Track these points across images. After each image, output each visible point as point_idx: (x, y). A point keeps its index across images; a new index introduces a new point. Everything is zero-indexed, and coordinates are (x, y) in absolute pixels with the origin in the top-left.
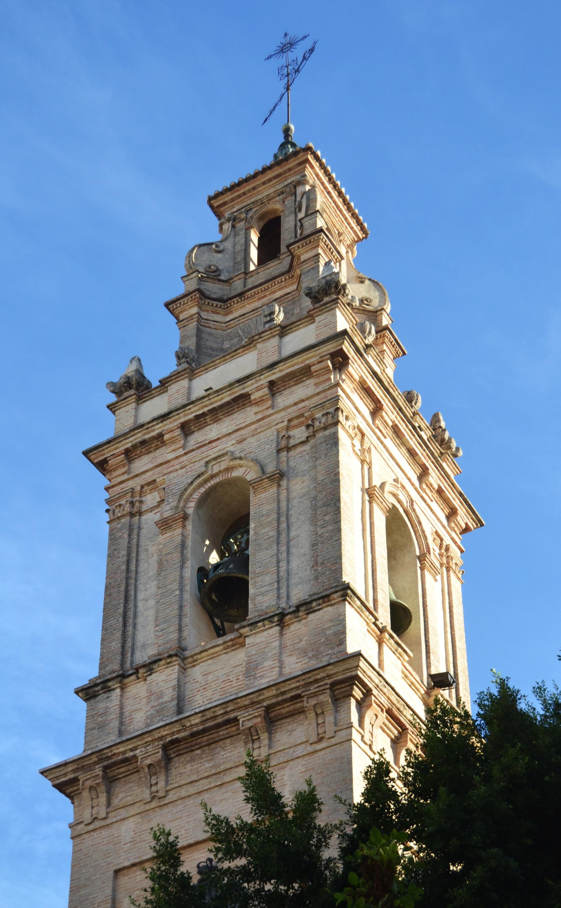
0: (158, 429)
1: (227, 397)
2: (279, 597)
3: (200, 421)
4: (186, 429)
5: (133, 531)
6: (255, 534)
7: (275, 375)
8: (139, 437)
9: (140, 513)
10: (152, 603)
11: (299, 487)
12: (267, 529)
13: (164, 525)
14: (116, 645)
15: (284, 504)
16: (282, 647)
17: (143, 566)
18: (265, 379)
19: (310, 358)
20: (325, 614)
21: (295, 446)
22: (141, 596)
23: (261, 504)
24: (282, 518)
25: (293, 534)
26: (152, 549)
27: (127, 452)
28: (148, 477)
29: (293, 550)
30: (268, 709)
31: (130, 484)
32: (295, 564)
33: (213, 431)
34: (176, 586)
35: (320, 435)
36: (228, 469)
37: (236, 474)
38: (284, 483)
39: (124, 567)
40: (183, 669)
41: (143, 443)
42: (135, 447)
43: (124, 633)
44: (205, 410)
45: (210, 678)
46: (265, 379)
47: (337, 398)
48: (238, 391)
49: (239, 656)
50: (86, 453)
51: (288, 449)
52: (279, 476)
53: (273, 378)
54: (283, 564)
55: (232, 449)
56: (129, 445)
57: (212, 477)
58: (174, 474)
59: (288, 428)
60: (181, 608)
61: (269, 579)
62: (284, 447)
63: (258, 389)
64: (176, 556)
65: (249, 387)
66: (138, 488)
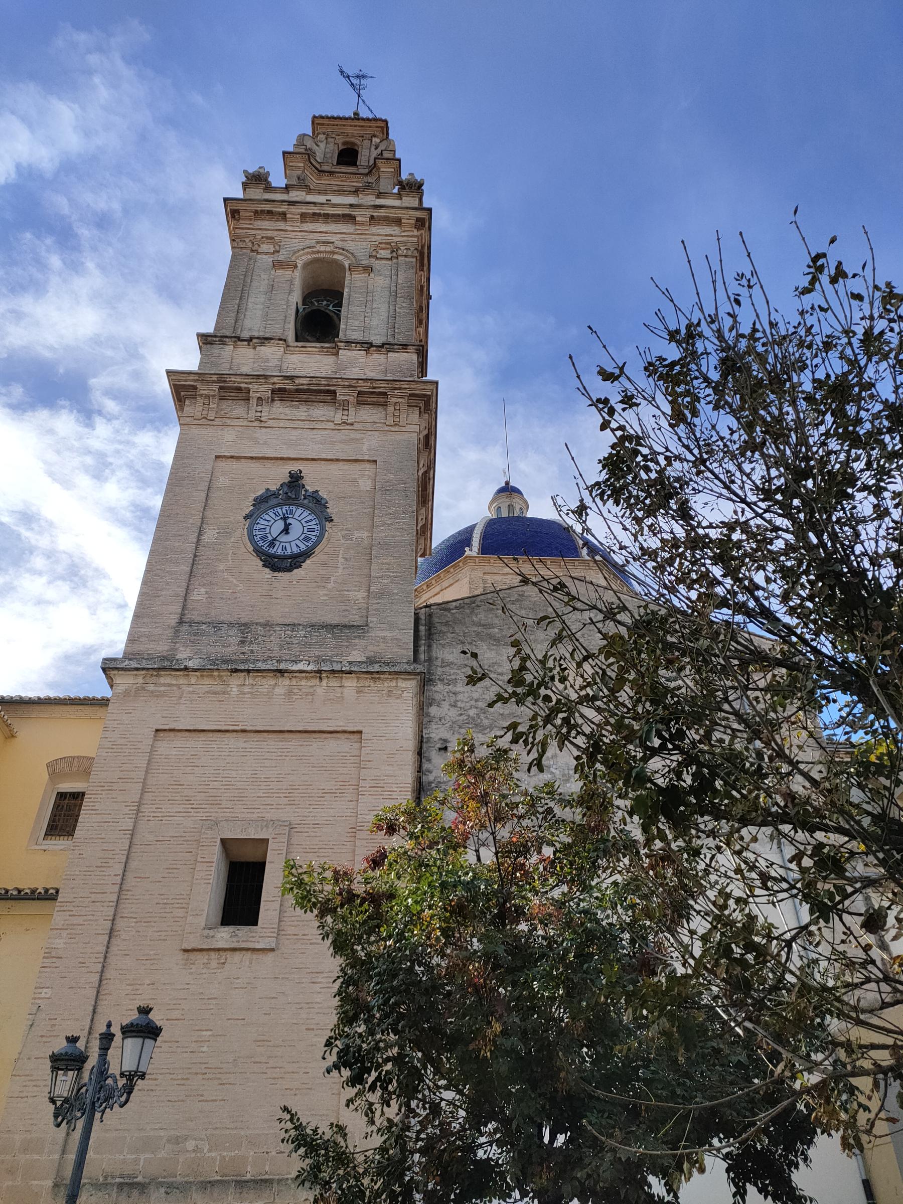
4: (304, 216)
18: (369, 213)
27: (256, 212)
37: (336, 257)
42: (262, 212)
57: (319, 252)
63: (362, 216)
65: (356, 212)
66: (259, 237)
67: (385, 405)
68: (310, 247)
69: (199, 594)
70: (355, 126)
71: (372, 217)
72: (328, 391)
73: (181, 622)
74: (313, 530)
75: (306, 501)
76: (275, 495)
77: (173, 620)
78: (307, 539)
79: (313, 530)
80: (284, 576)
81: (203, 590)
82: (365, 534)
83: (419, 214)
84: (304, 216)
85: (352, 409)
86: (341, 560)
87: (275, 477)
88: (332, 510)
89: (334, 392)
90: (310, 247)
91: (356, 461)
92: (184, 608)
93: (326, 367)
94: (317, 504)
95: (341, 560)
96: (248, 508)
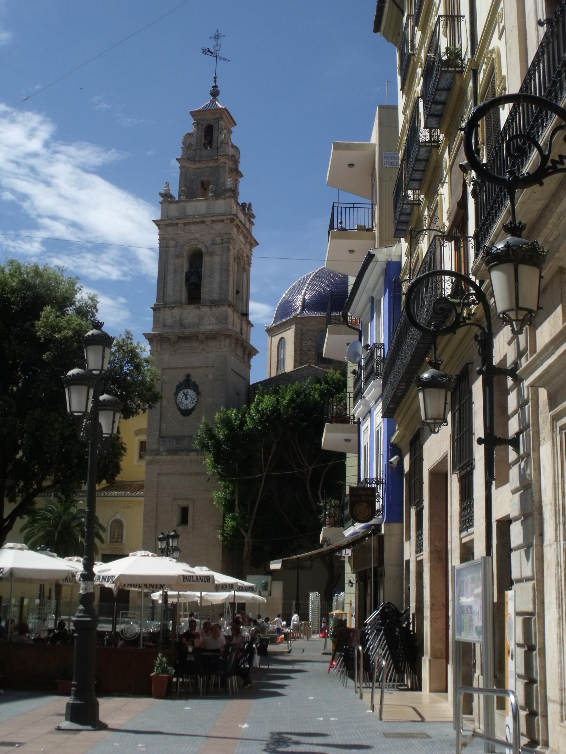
0: (176, 221)
1: (198, 220)
3: (189, 223)
5: (166, 253)
7: (214, 219)
8: (170, 222)
10: (172, 282)
11: (217, 259)
13: (177, 257)
18: (210, 219)
21: (217, 244)
22: (169, 278)
23: (206, 260)
27: (166, 225)
31: (166, 236)
33: (193, 228)
35: (225, 244)
36: (197, 245)
41: (171, 224)
42: (168, 224)
46: (210, 219)
48: (202, 219)
49: (197, 312)
51: (215, 244)
57: (192, 245)
59: (216, 237)
60: (181, 288)
63: (208, 221)
67: (216, 339)
69: (164, 426)
71: (212, 220)
73: (160, 437)
74: (194, 399)
77: (157, 437)
78: (193, 403)
79: (194, 399)
80: (187, 418)
81: (164, 425)
84: (185, 224)
85: (205, 343)
87: (181, 378)
88: (200, 389)
89: (198, 336)
91: (207, 366)
92: (160, 432)
94: (195, 388)
96: (174, 390)
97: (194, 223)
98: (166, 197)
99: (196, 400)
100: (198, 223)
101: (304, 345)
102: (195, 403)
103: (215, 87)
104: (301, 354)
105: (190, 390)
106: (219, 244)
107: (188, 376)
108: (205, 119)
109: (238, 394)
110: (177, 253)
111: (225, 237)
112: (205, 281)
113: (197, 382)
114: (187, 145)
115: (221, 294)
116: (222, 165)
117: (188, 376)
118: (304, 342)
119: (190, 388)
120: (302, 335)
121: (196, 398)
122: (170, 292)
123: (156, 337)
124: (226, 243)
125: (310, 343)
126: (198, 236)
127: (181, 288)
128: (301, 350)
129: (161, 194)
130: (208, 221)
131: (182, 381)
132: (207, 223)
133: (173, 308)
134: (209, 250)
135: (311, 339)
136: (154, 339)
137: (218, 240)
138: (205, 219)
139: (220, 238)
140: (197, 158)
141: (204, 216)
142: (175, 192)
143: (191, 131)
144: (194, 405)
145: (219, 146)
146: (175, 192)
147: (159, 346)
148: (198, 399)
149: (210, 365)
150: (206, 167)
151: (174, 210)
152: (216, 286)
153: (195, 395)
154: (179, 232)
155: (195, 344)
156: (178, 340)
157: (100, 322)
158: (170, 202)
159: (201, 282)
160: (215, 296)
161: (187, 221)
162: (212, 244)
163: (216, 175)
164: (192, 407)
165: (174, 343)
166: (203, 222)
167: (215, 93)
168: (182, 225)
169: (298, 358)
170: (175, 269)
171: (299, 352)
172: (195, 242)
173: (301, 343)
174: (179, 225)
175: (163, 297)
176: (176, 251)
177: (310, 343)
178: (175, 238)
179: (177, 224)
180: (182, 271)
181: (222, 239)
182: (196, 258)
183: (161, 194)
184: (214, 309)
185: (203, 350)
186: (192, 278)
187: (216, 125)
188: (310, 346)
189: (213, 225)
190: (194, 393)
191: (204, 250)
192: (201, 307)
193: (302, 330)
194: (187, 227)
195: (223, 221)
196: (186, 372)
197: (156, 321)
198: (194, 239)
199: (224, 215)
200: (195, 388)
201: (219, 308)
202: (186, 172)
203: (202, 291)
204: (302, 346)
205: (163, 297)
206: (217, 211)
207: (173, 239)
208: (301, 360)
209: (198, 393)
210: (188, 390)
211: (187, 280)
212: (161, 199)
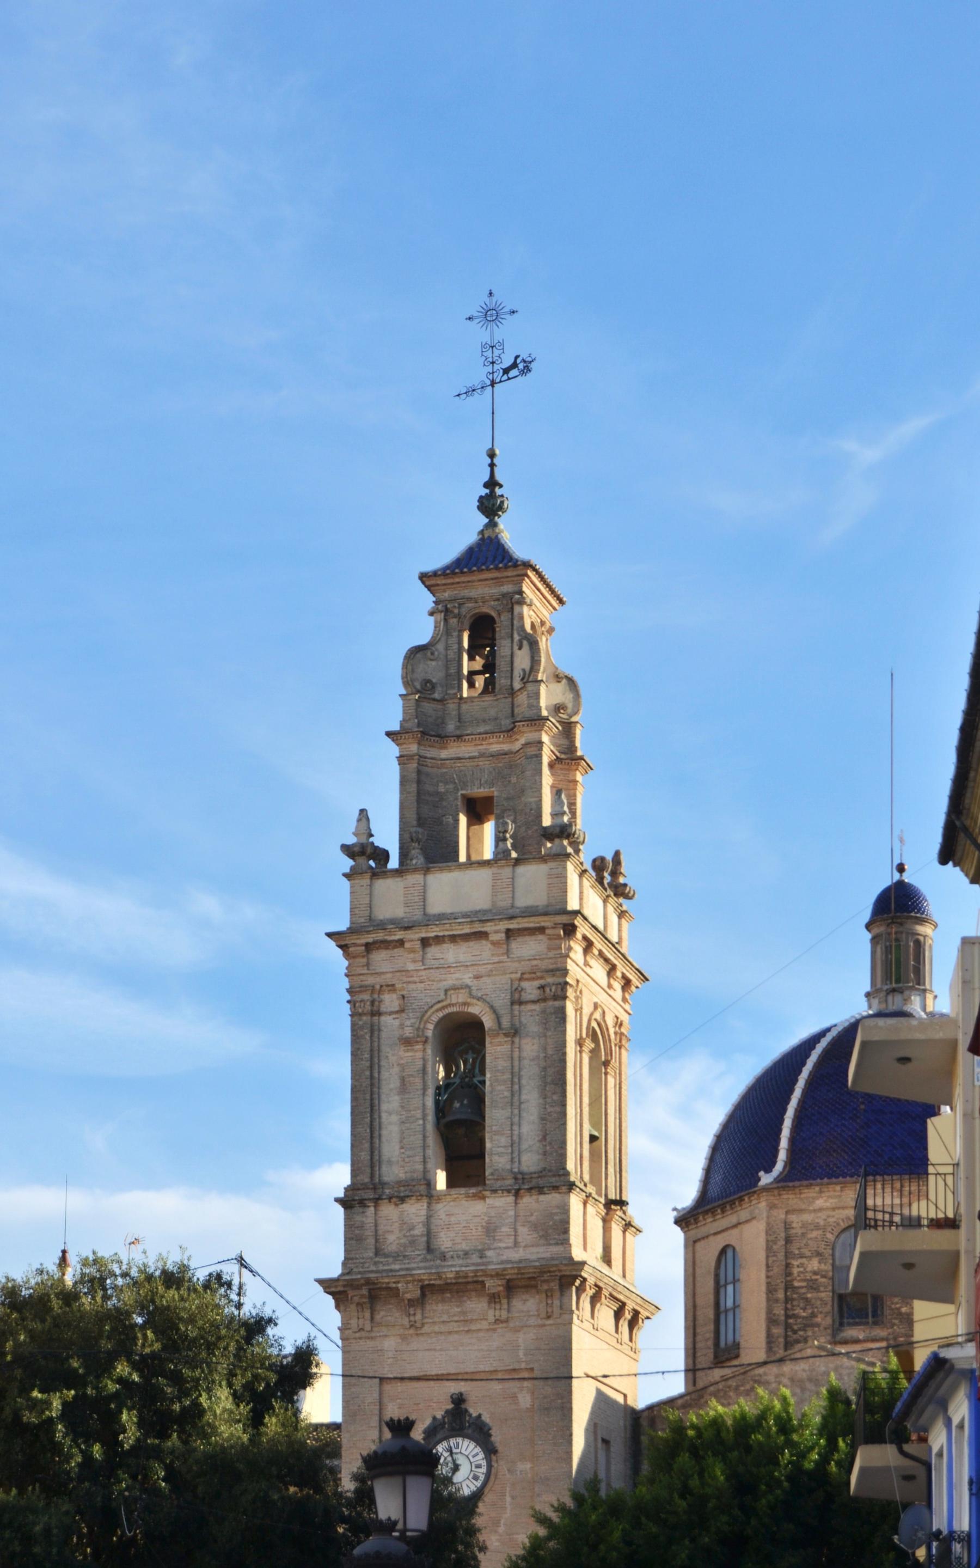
0: (399, 935)
1: (467, 930)
2: (512, 1160)
3: (439, 940)
4: (425, 942)
5: (374, 1030)
6: (491, 1085)
7: (513, 925)
8: (380, 936)
9: (379, 1014)
10: (394, 1118)
11: (530, 1047)
12: (502, 1087)
13: (407, 1042)
14: (365, 1156)
15: (516, 1063)
16: (516, 1216)
17: (385, 1075)
19: (545, 922)
20: (551, 1199)
21: (527, 1002)
22: (384, 1107)
23: (496, 1051)
24: (515, 1076)
25: (524, 1097)
26: (393, 1059)
28: (388, 978)
29: (524, 1114)
30: (508, 1281)
31: (370, 980)
32: (525, 1129)
33: (451, 953)
34: (419, 1114)
35: (551, 1003)
36: (465, 1004)
38: (517, 1040)
39: (368, 1073)
40: (429, 1204)
42: (375, 943)
43: (372, 1143)
44: (447, 933)
45: (453, 1219)
47: (565, 972)
48: (478, 927)
49: (478, 1207)
50: (329, 935)
52: (514, 1032)
53: (511, 926)
54: (516, 1128)
55: (468, 982)
56: (370, 940)
57: (450, 1005)
58: (412, 986)
59: (521, 979)
60: (424, 1137)
61: (504, 1140)
62: (517, 1001)
63: (497, 932)
64: (418, 1081)
65: (488, 927)
66: (378, 987)
68: (439, 1002)
70: (486, 580)
72: (476, 1282)
74: (479, 1466)
75: (470, 1431)
76: (442, 1424)
79: (479, 1466)
82: (529, 1466)
83: (564, 919)
84: (425, 942)
86: (508, 1499)
88: (497, 1437)
89: (483, 1283)
90: (439, 1002)
93: (477, 1220)
94: (481, 1434)
95: (508, 1499)
97: (454, 939)
98: (365, 857)
99: (484, 1470)
100: (466, 937)
101: (795, 1271)
102: (482, 1477)
103: (492, 484)
104: (787, 1300)
105: (466, 1442)
106: (534, 1002)
107: (459, 1400)
108: (469, 599)
109: (606, 1442)
110: (408, 1032)
111: (550, 980)
112: (495, 1116)
113: (486, 1418)
114: (418, 687)
115: (545, 1153)
116: (532, 751)
117: (459, 1400)
118: (795, 1263)
119: (465, 1436)
120: (788, 1240)
121: (484, 1463)
122: (391, 1148)
123: (358, 1287)
124: (555, 998)
125: (814, 1264)
126: (467, 978)
127: (424, 1137)
128: (788, 1286)
129: (348, 850)
130: (497, 932)
131: (439, 1415)
132: (493, 937)
133: (402, 1200)
134: (506, 1022)
135: (818, 1254)
136: (351, 1293)
137: (530, 989)
138: (488, 927)
139: (537, 983)
140: (451, 727)
141: (481, 916)
142: (387, 836)
143: (424, 639)
144: (479, 1484)
145: (517, 685)
146: (387, 836)
147: (367, 1314)
148: (490, 1467)
149: (523, 1366)
150: (482, 755)
151: (392, 898)
152: (529, 1128)
153: (481, 1455)
154: (411, 966)
155: (476, 1306)
156: (423, 1295)
157: (396, 1419)
158: (375, 875)
159: (483, 1117)
160: (530, 1161)
161: (431, 931)
162: (512, 1003)
163: (514, 780)
164: (474, 1488)
165: (411, 1303)
166: (482, 935)
167: (490, 506)
168: (418, 945)
169: (779, 1311)
170: (403, 1080)
171: (781, 1295)
172: (458, 998)
173: (788, 1265)
174: (407, 945)
175: (372, 1167)
176: (402, 1026)
177: (814, 1264)
178: (398, 986)
179: (401, 943)
180: (425, 1089)
181: (542, 987)
182: (462, 1038)
183: (348, 850)
184: (528, 1201)
185: (497, 1321)
186: (457, 1105)
187: (505, 617)
188: (815, 1273)
189: (514, 945)
190: (478, 1449)
191: (488, 1022)
192: (487, 1193)
193: (787, 1226)
194: (433, 951)
195: (541, 930)
196: (454, 1388)
197: (353, 1237)
198: (455, 988)
199: (546, 914)
200: (481, 1434)
201: (542, 1198)
202: (419, 772)
203: (488, 1145)
204: (790, 1274)
205: (372, 1167)
206: (523, 901)
207: (392, 988)
208: (787, 1317)
209: (490, 1451)
210: (460, 1440)
211: (441, 1110)
212: (347, 864)
